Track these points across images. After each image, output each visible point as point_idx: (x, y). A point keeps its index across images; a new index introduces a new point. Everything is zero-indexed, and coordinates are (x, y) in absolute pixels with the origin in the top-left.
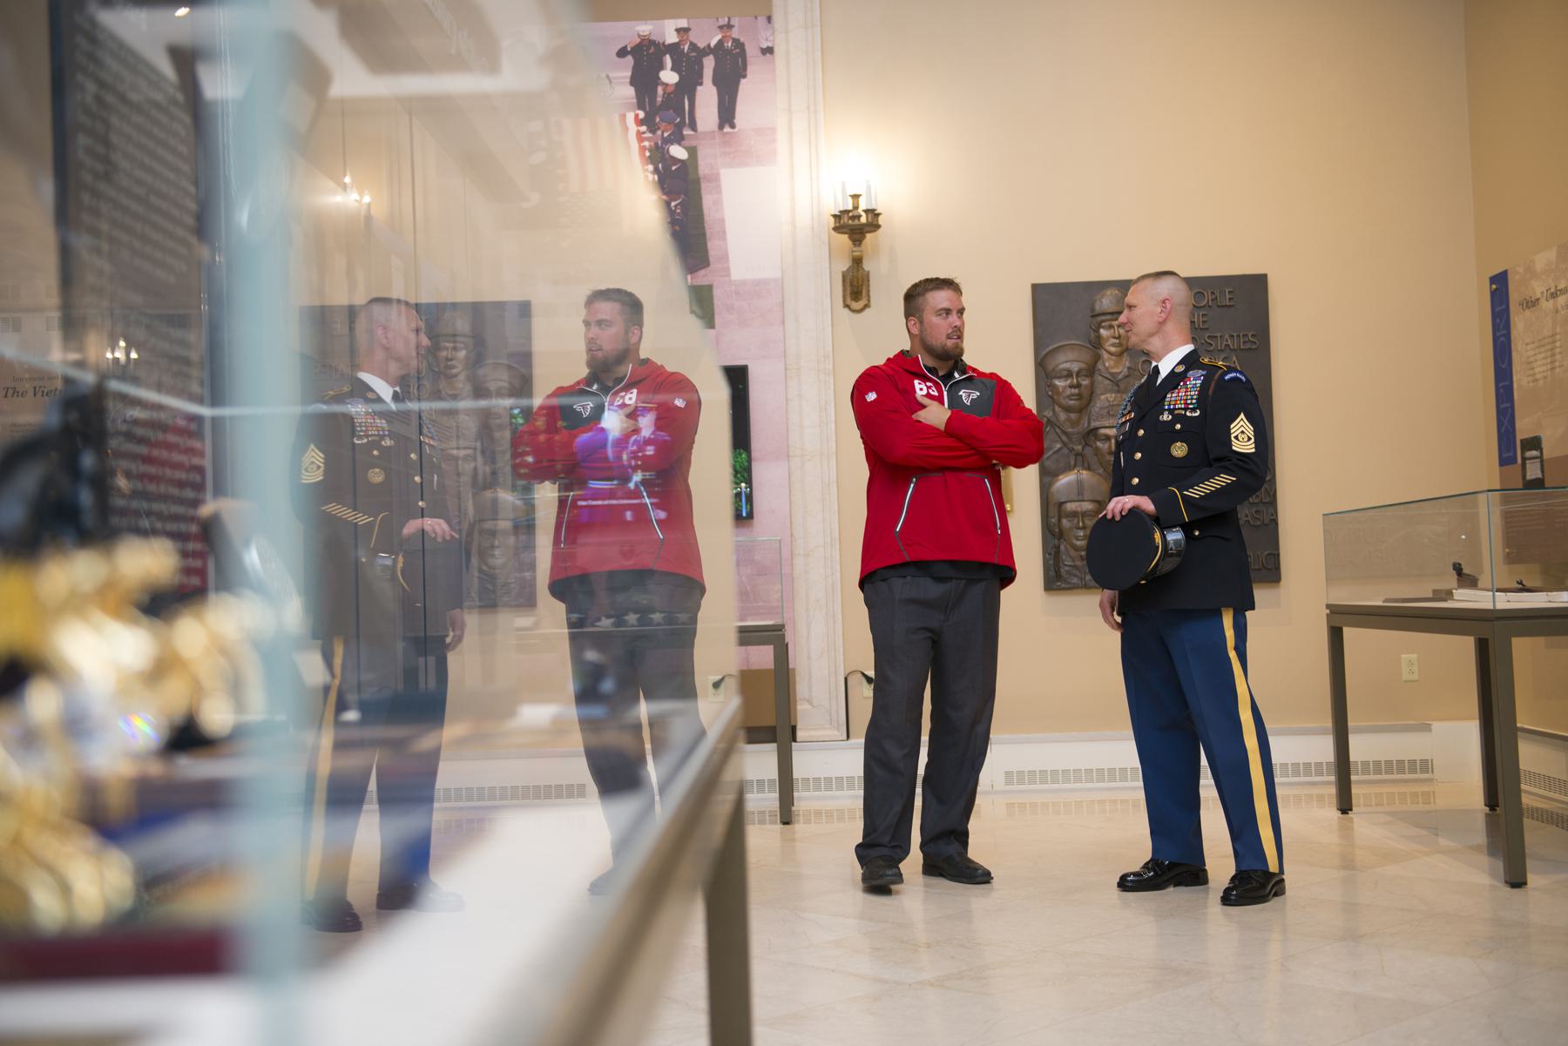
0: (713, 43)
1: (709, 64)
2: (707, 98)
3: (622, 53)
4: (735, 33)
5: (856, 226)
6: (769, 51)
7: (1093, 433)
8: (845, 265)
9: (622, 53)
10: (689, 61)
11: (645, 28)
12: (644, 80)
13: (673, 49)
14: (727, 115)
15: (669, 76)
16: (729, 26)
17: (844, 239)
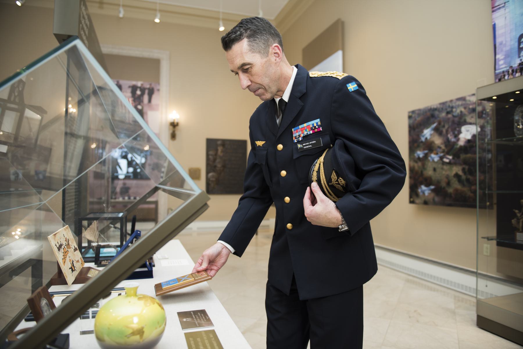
0: (148, 86)
1: (147, 91)
2: (146, 98)
3: (129, 87)
4: (153, 86)
5: (174, 125)
6: (158, 90)
7: (215, 167)
8: (171, 131)
9: (129, 87)
10: (143, 90)
11: (134, 83)
12: (133, 92)
13: (140, 88)
14: (150, 101)
15: (139, 92)
16: (151, 85)
17: (171, 127)
